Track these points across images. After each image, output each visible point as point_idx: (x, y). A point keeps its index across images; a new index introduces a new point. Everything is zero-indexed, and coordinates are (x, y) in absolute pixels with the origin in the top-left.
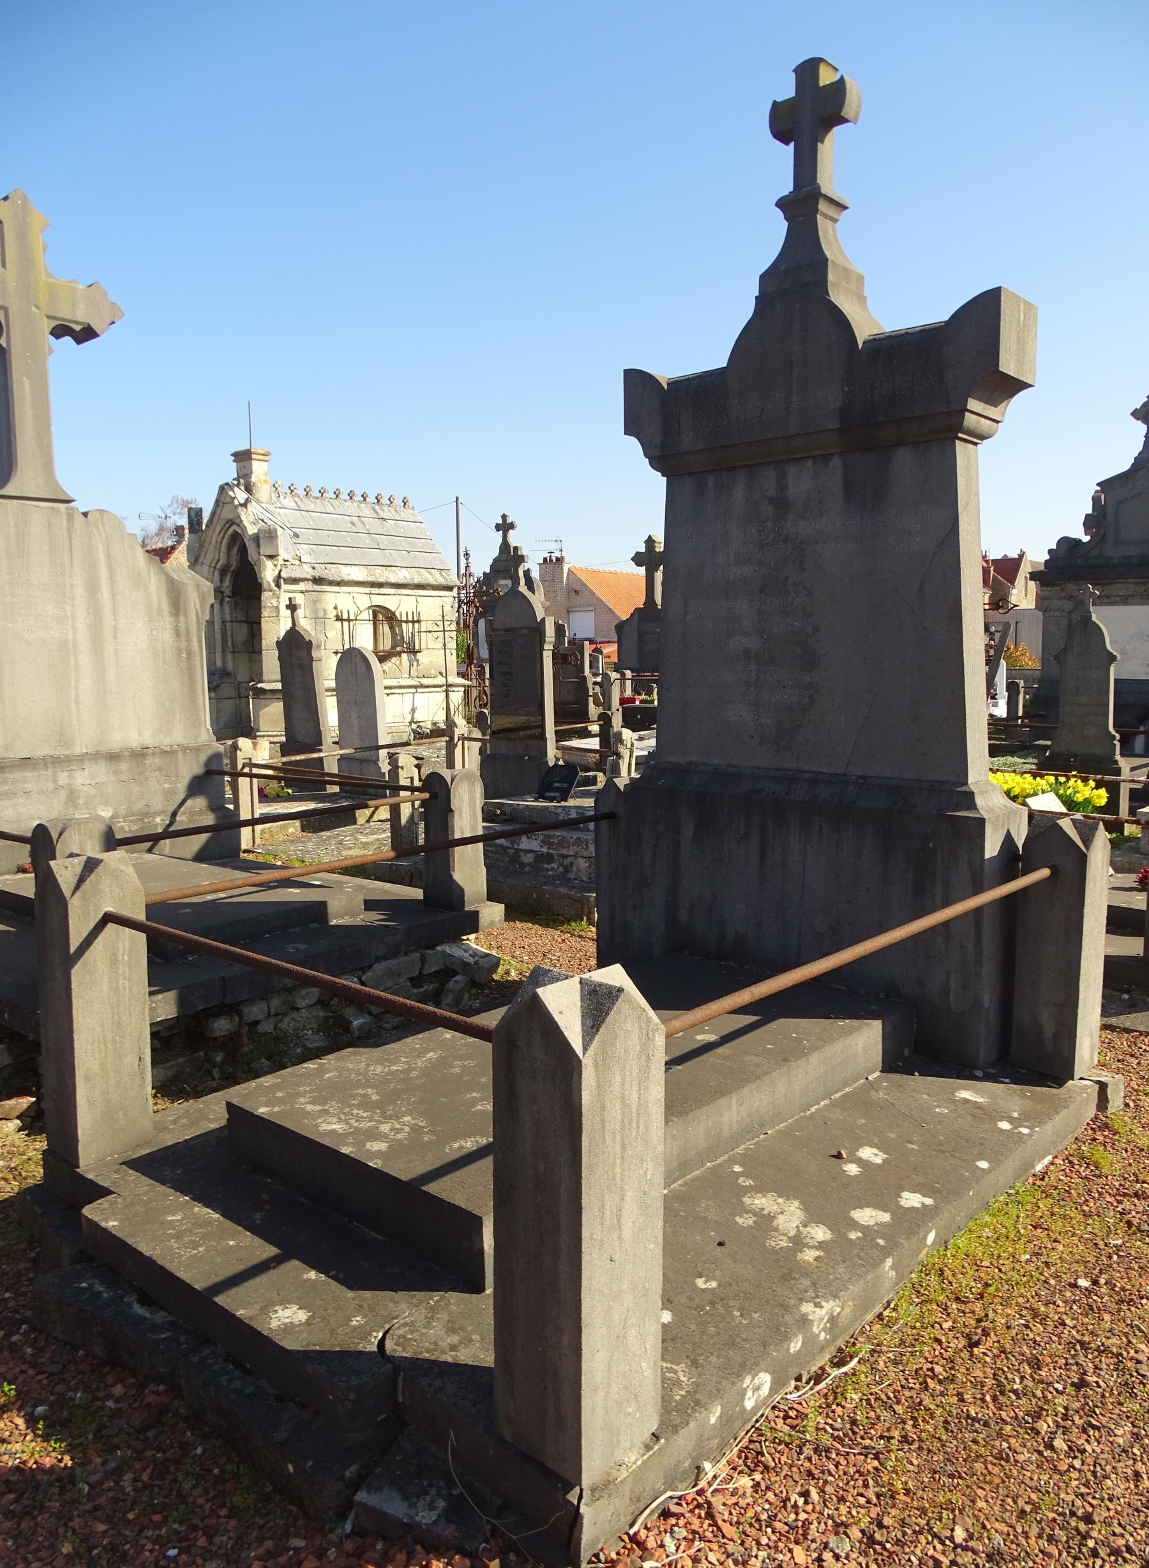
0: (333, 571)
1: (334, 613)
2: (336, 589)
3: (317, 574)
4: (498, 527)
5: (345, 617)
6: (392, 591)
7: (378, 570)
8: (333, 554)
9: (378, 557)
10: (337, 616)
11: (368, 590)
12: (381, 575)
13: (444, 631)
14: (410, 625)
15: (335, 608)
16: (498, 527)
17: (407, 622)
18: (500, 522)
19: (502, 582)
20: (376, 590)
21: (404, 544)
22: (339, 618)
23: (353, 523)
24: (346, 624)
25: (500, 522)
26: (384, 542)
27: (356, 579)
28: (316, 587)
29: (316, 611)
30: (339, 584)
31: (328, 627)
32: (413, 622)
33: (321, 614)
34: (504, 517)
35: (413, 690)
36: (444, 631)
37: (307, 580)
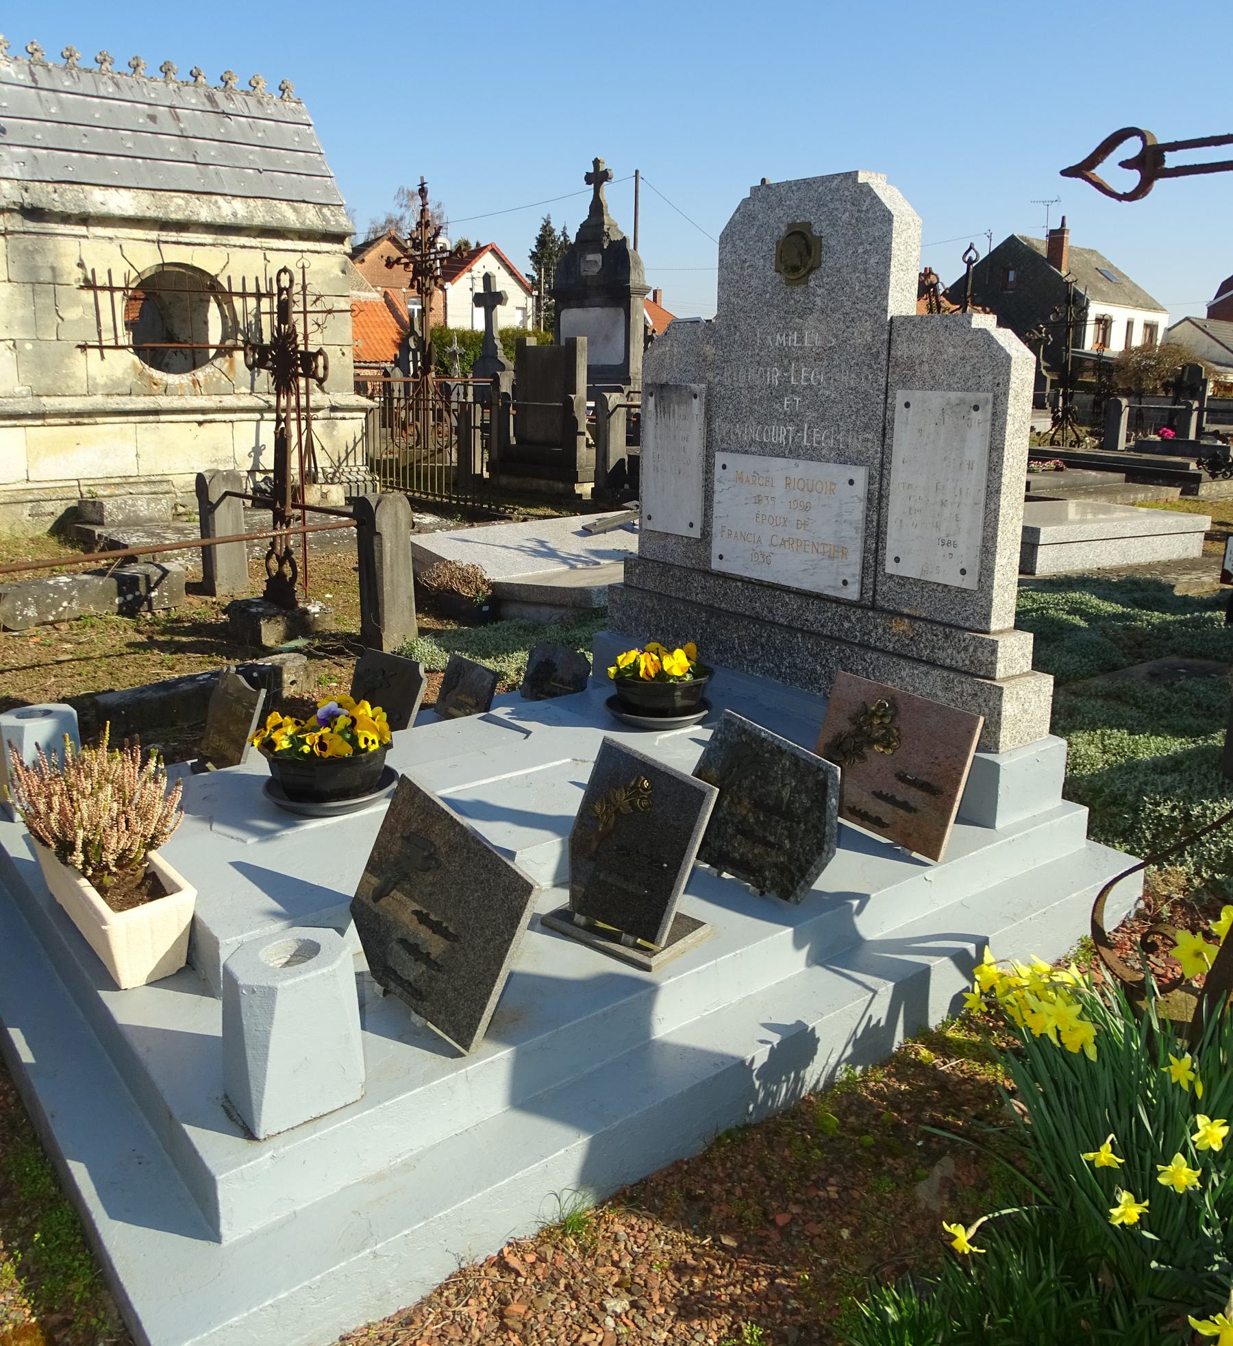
0: (69, 196)
1: (78, 273)
2: (81, 230)
3: (28, 199)
4: (589, 179)
5: (102, 280)
6: (208, 238)
7: (179, 199)
8: (74, 165)
9: (189, 175)
10: (86, 280)
11: (153, 235)
12: (177, 206)
13: (305, 312)
14: (251, 302)
15: (81, 265)
16: (589, 179)
17: (244, 295)
18: (591, 170)
19: (590, 257)
20: (173, 236)
21: (254, 156)
22: (89, 285)
23: (153, 118)
24: (104, 297)
25: (591, 170)
26: (210, 151)
27: (117, 212)
28: (31, 226)
29: (33, 269)
30: (85, 219)
31: (62, 301)
32: (259, 296)
33: (46, 276)
34: (596, 163)
35: (258, 416)
36: (305, 312)
37: (10, 211)
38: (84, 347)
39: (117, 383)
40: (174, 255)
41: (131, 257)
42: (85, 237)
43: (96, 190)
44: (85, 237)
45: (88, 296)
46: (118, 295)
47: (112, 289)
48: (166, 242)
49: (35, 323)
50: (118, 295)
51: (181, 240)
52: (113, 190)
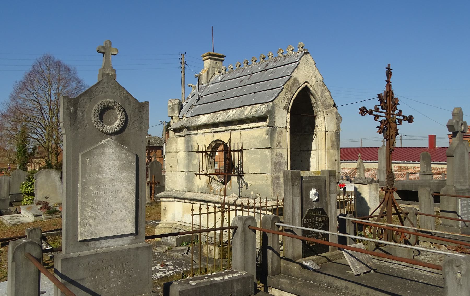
6: (223, 128)
20: (215, 129)
24: (201, 154)
38: (196, 174)
39: (203, 189)
40: (218, 136)
41: (204, 139)
42: (197, 134)
43: (202, 116)
44: (197, 134)
45: (198, 154)
46: (204, 154)
47: (202, 152)
48: (214, 132)
49: (188, 166)
50: (204, 154)
51: (217, 130)
52: (206, 115)
